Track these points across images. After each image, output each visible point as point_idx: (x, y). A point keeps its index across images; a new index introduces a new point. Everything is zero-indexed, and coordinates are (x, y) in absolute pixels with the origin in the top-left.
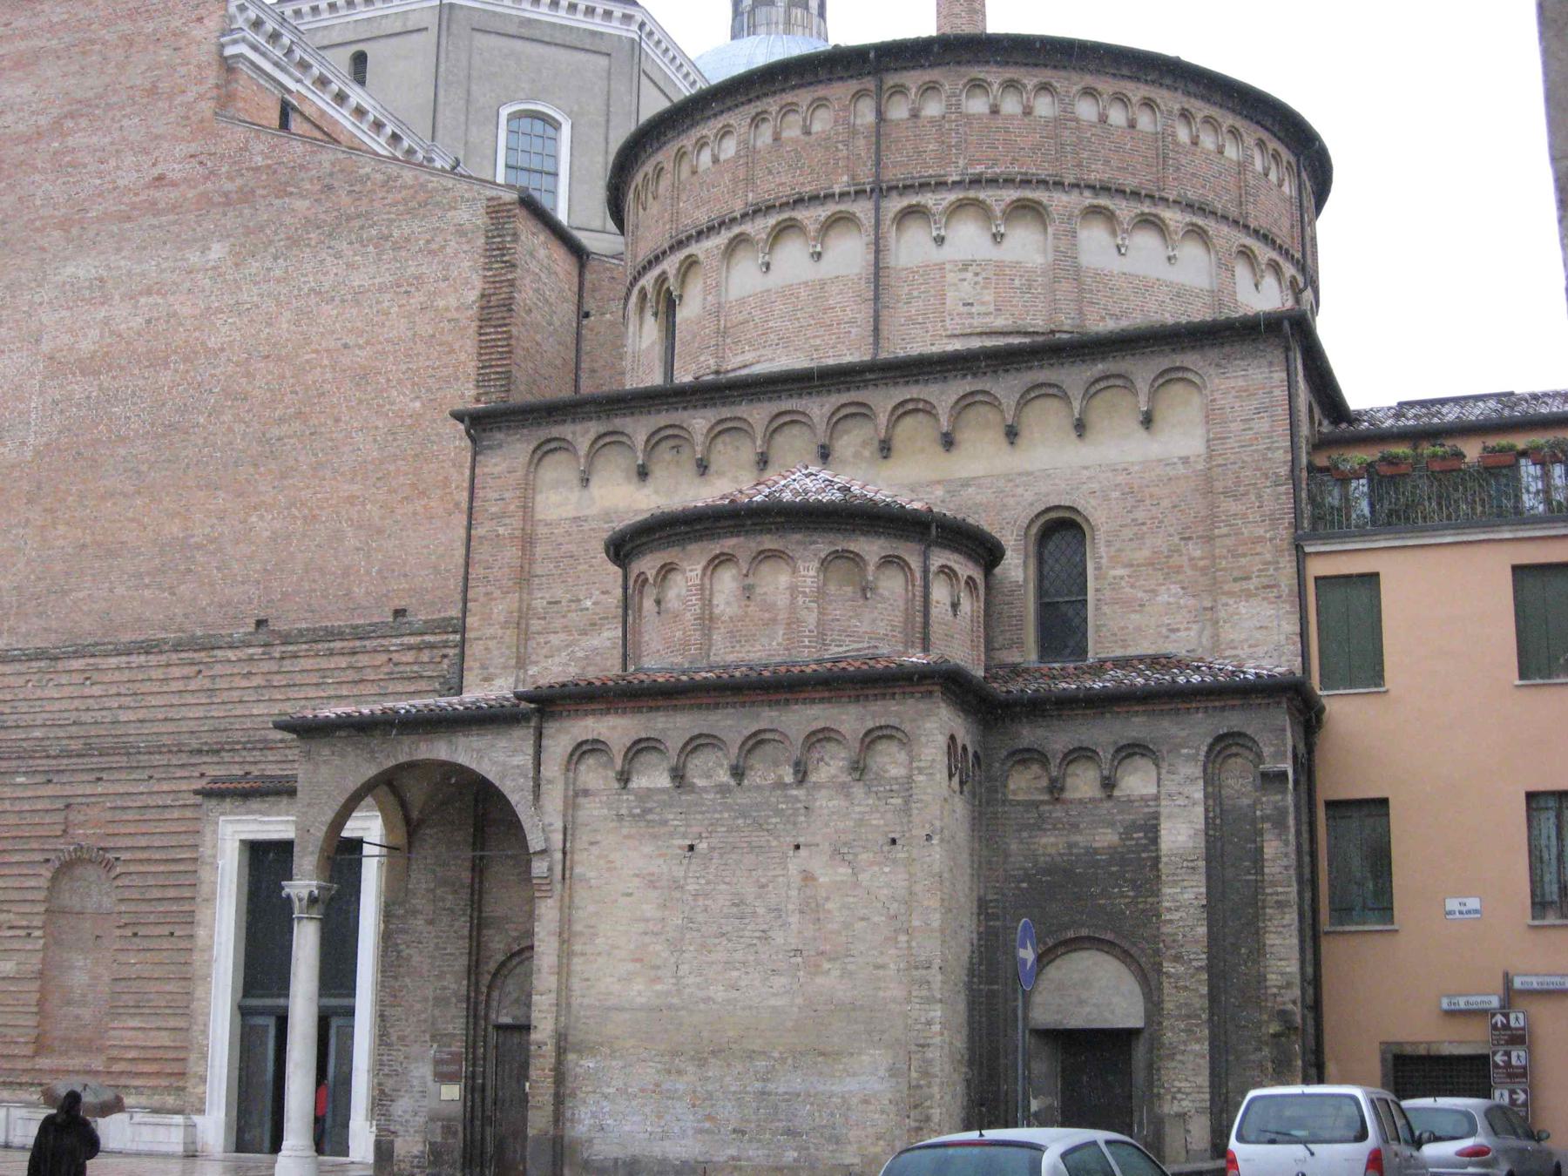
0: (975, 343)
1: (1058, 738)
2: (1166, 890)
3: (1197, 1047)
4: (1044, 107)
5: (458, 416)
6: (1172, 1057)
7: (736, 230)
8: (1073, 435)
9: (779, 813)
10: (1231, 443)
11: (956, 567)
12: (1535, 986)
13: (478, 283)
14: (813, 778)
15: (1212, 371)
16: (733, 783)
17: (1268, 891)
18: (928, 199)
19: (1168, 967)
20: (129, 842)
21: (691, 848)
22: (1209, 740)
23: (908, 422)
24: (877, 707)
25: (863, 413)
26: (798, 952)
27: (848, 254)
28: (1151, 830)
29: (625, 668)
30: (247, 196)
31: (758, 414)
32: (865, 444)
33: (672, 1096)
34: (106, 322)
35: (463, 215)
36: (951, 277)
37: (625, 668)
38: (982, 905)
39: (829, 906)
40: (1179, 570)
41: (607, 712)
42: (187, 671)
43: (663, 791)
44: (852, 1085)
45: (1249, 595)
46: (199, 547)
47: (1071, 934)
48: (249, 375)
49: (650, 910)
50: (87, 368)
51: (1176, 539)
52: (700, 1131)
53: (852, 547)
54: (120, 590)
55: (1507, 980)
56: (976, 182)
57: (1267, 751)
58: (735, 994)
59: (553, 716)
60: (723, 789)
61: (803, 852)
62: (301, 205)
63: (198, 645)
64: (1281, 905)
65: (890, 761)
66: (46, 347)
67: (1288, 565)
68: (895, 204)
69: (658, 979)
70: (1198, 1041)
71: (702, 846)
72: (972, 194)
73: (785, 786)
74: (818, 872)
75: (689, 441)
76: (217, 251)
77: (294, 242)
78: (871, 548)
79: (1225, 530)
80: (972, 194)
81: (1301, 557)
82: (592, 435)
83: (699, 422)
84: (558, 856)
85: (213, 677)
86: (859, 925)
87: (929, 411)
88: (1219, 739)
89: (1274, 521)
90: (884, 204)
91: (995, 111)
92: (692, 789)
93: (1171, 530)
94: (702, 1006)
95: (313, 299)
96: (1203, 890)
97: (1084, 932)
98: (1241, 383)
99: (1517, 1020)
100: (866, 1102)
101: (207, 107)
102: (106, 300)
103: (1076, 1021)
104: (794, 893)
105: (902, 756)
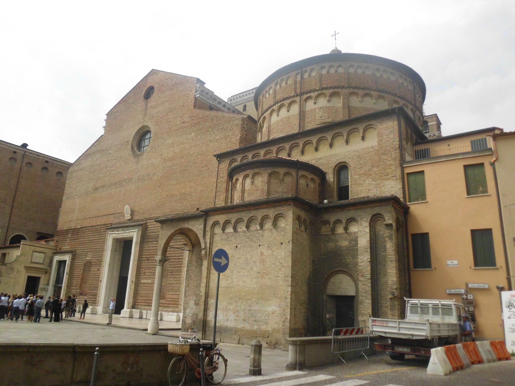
1: (332, 218)
2: (360, 257)
3: (368, 301)
5: (215, 156)
6: (361, 304)
8: (345, 144)
9: (256, 237)
10: (384, 141)
11: (307, 175)
12: (476, 287)
13: (239, 135)
14: (264, 228)
15: (378, 124)
16: (246, 230)
17: (389, 257)
18: (312, 94)
19: (361, 278)
20: (172, 255)
21: (237, 247)
22: (371, 216)
24: (278, 208)
27: (295, 109)
28: (356, 241)
33: (229, 310)
35: (237, 122)
36: (317, 111)
38: (313, 261)
39: (267, 261)
40: (371, 175)
41: (220, 214)
43: (232, 233)
44: (270, 309)
45: (389, 179)
46: (188, 194)
47: (336, 269)
51: (370, 167)
52: (235, 320)
53: (277, 170)
54: (173, 204)
55: (467, 285)
57: (386, 218)
58: (244, 284)
59: (209, 216)
61: (261, 247)
62: (208, 124)
64: (391, 261)
66: (163, 157)
67: (399, 171)
68: (305, 96)
69: (228, 280)
70: (368, 299)
71: (239, 246)
72: (322, 92)
73: (258, 230)
74: (264, 252)
76: (193, 134)
77: (206, 131)
78: (282, 171)
79: (382, 163)
80: (322, 92)
81: (403, 169)
82: (241, 157)
84: (208, 249)
86: (273, 266)
88: (374, 216)
89: (395, 159)
90: (302, 97)
93: (369, 165)
94: (237, 287)
96: (369, 257)
97: (339, 269)
98: (386, 126)
99: (470, 297)
100: (273, 313)
102: (174, 147)
103: (338, 293)
104: (259, 258)
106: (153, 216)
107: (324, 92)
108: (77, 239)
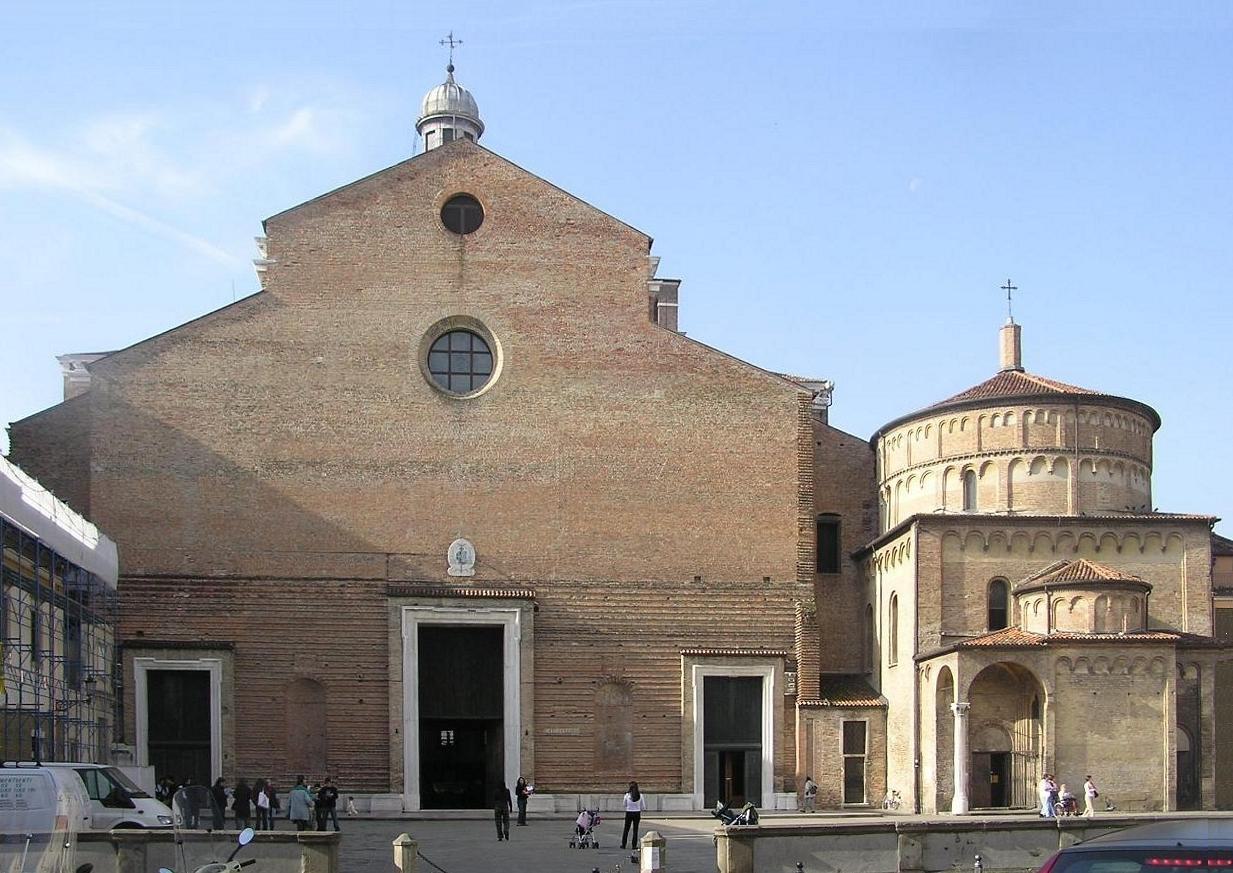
0: (1111, 516)
4: (1124, 426)
7: (1017, 456)
14: (1134, 672)
23: (1083, 540)
25: (1070, 535)
26: (1129, 727)
28: (1197, 689)
29: (1049, 632)
30: (671, 369)
31: (1032, 531)
32: (1069, 546)
34: (596, 421)
37: (1049, 632)
42: (661, 598)
48: (682, 459)
49: (1081, 713)
50: (588, 442)
56: (1108, 453)
60: (1106, 675)
63: (665, 589)
65: (1159, 668)
66: (562, 427)
71: (1099, 693)
75: (1005, 537)
76: (657, 394)
77: (699, 396)
82: (967, 531)
83: (1010, 531)
85: (676, 602)
87: (1092, 537)
91: (1112, 425)
92: (1094, 674)
95: (712, 427)
101: (644, 317)
105: (1161, 666)
106: (553, 576)
107: (1108, 458)
108: (230, 611)
